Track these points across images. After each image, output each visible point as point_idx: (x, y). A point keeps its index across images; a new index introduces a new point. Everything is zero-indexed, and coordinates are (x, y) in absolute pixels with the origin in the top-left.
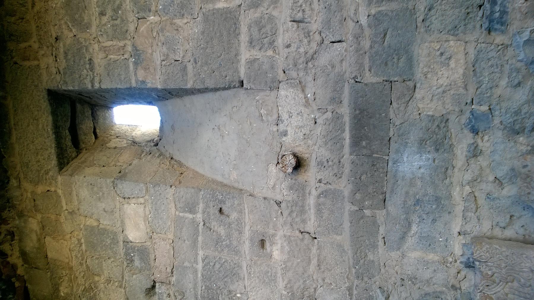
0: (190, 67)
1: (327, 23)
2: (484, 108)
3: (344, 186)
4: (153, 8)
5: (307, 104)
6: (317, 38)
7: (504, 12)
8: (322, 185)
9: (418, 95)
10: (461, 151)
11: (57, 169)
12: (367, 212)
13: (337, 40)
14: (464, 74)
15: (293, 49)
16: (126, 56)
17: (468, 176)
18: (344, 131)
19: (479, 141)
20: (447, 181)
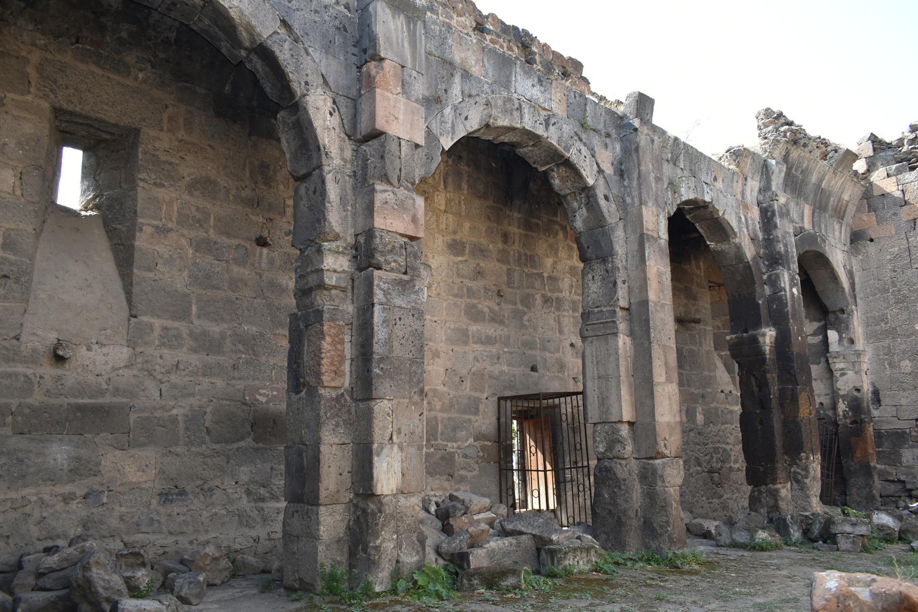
0: (151, 275)
1: (174, 387)
2: (105, 500)
3: (36, 398)
4: (197, 254)
5: (114, 369)
6: (165, 379)
7: (171, 501)
8: (38, 379)
9: (118, 452)
10: (68, 488)
11: (57, 105)
12: (9, 419)
13: (164, 394)
14: (131, 483)
15: (159, 361)
16: (164, 220)
17: (46, 497)
18: (90, 398)
19: (78, 501)
20: (40, 482)
